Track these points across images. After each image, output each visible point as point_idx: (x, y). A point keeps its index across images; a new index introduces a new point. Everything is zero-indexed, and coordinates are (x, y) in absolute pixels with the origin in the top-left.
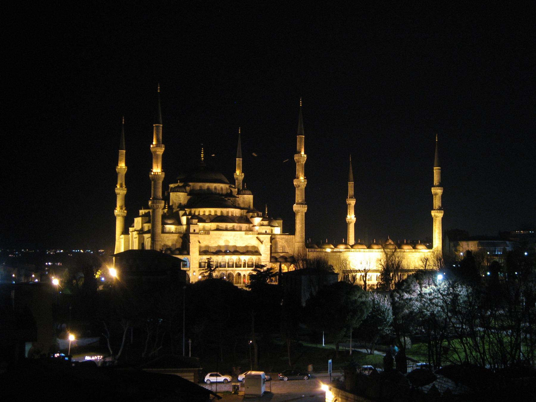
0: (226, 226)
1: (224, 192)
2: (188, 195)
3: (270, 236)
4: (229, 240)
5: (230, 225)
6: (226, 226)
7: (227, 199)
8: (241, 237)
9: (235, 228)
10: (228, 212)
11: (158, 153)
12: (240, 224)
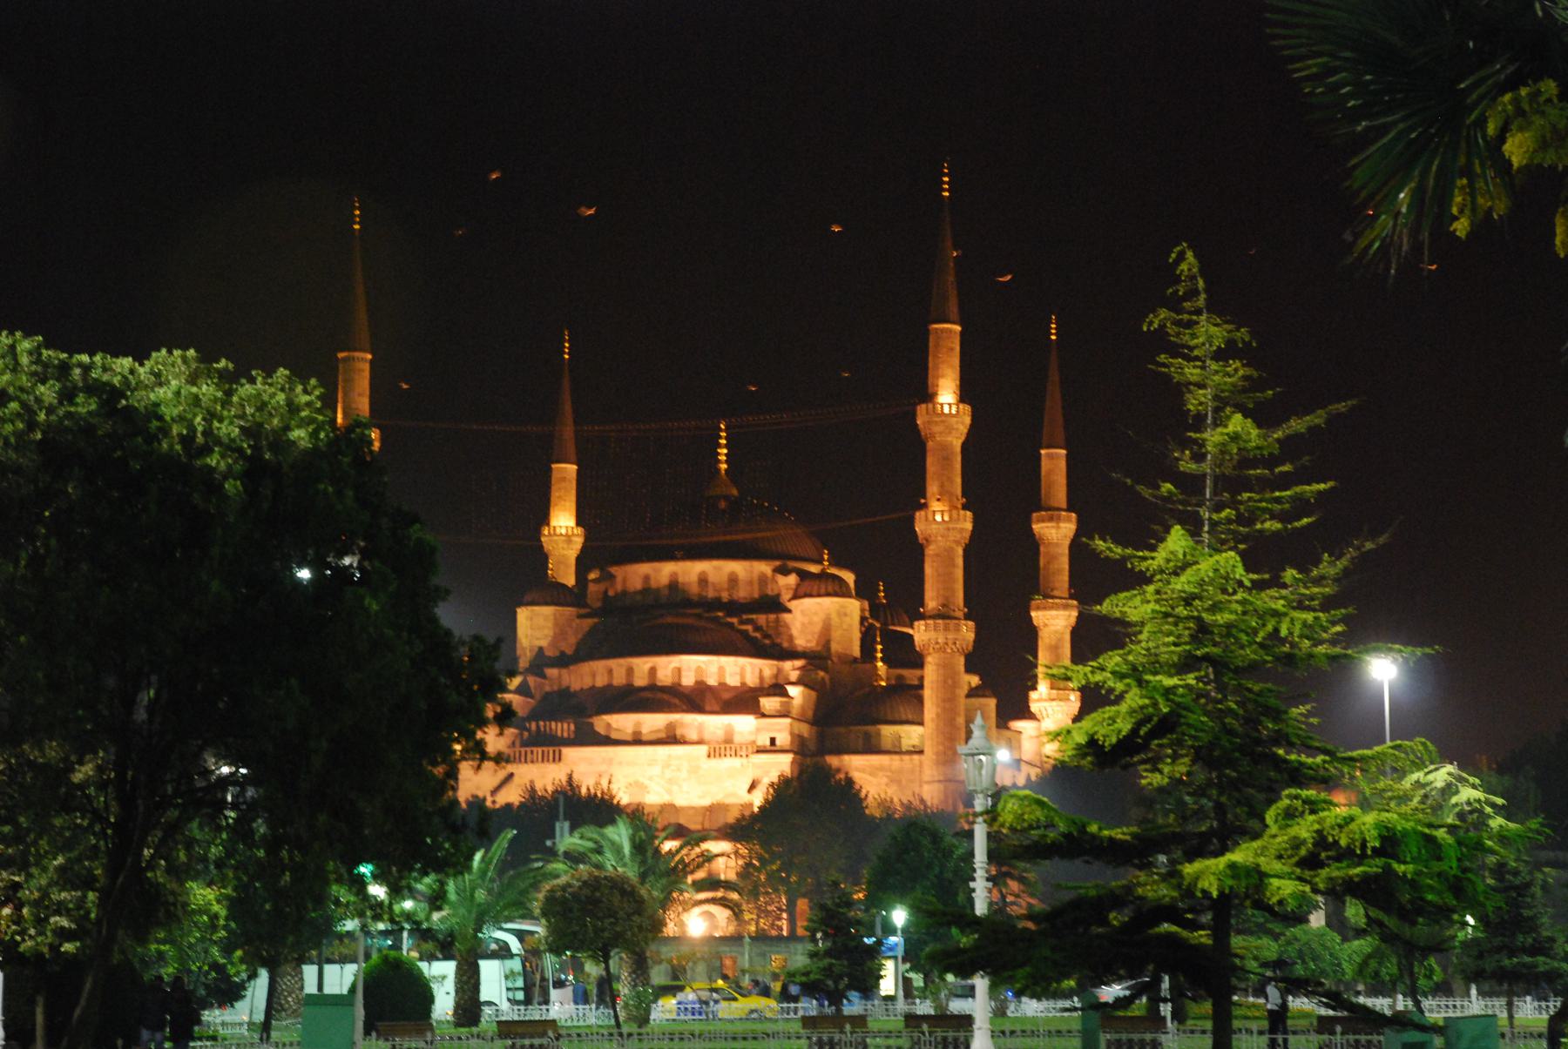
1: (742, 594)
2: (580, 616)
4: (647, 782)
5: (653, 722)
6: (638, 724)
7: (735, 620)
8: (694, 770)
9: (645, 730)
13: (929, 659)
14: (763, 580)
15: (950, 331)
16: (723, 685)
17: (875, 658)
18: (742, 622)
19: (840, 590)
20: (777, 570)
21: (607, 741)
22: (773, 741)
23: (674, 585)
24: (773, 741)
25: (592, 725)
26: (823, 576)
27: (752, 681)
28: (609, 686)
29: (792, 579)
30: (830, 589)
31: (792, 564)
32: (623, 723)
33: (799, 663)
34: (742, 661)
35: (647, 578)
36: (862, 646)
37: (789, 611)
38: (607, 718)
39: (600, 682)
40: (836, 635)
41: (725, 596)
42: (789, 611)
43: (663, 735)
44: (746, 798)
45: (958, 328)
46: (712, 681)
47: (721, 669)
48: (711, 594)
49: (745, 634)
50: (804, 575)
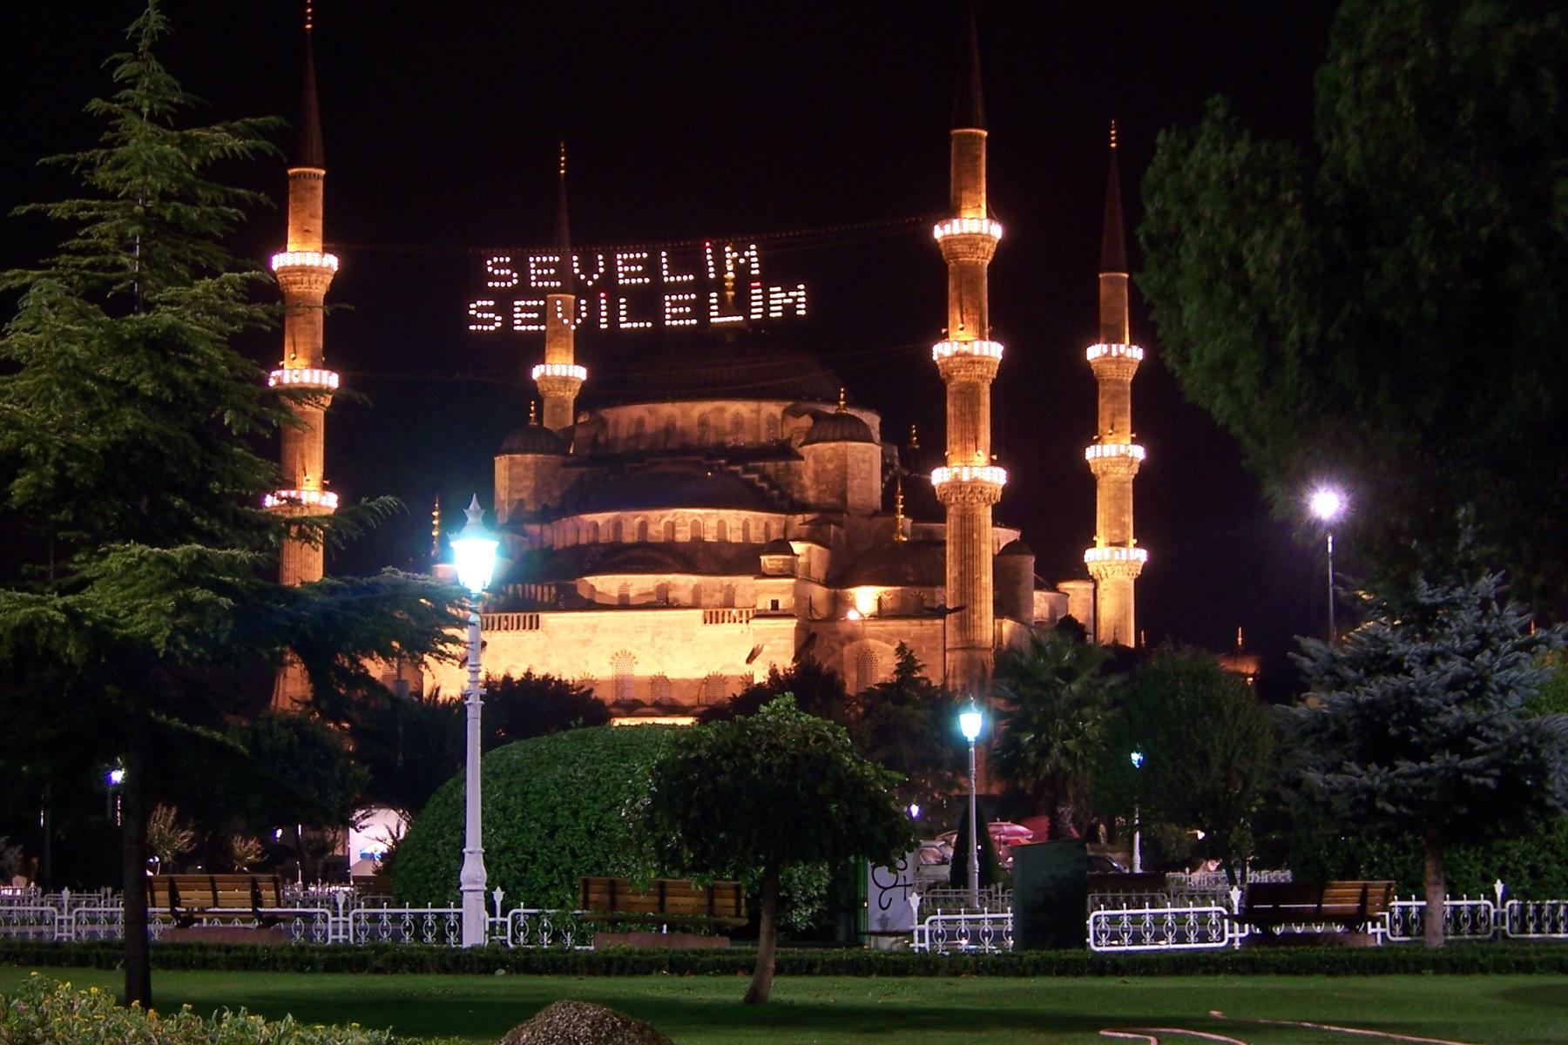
0: (625, 586)
1: (745, 439)
2: (565, 465)
3: (791, 624)
4: (635, 652)
5: (641, 583)
6: (625, 586)
7: (739, 468)
10: (672, 527)
11: (295, 289)
12: (726, 580)
13: (951, 510)
14: (772, 422)
15: (976, 135)
16: (723, 543)
17: (896, 510)
18: (746, 471)
19: (859, 433)
20: (786, 412)
21: (591, 605)
22: (775, 604)
23: (669, 430)
24: (775, 604)
25: (575, 588)
26: (838, 418)
27: (756, 536)
28: (595, 544)
29: (806, 421)
30: (846, 434)
31: (804, 405)
32: (607, 584)
33: (809, 517)
34: (745, 514)
35: (641, 422)
36: (883, 497)
37: (802, 458)
38: (590, 579)
39: (583, 540)
40: (854, 484)
41: (730, 441)
42: (802, 458)
43: (654, 599)
44: (746, 669)
45: (985, 133)
46: (710, 537)
47: (721, 524)
48: (712, 438)
49: (751, 483)
50: (817, 417)
